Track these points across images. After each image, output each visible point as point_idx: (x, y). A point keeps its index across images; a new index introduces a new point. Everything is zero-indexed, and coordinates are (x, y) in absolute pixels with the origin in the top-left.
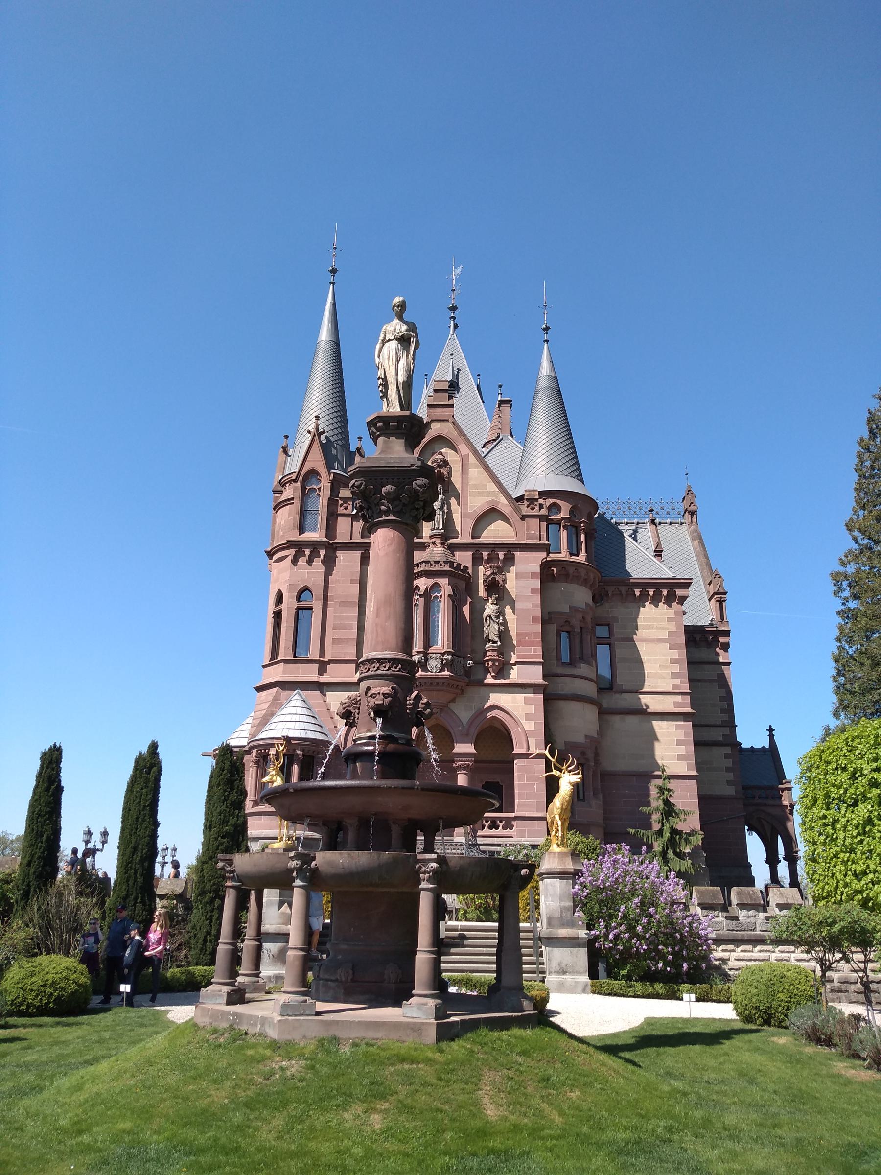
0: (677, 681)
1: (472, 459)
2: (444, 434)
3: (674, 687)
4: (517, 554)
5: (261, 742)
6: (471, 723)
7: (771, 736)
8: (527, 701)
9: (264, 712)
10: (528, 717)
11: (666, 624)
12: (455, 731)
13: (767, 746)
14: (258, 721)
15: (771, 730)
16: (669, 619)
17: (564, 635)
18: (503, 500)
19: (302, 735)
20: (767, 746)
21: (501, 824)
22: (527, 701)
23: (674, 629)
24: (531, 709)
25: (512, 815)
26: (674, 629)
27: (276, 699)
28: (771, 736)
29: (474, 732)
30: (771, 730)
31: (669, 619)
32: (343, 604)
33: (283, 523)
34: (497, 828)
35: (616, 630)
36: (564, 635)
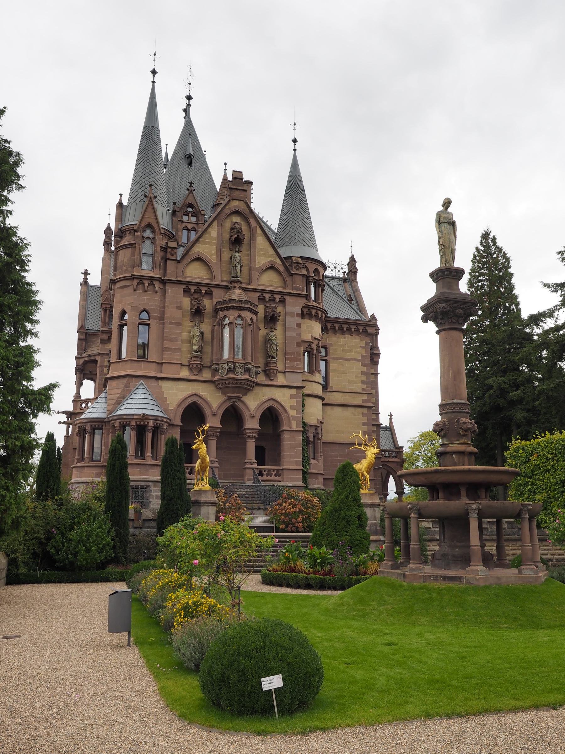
0: (365, 386)
1: (259, 231)
2: (240, 210)
3: (363, 390)
4: (288, 298)
5: (124, 417)
6: (258, 409)
7: (391, 419)
8: (292, 396)
9: (118, 396)
10: (292, 407)
11: (360, 350)
12: (246, 414)
13: (388, 425)
14: (114, 402)
15: (391, 415)
16: (362, 347)
17: (306, 354)
18: (278, 261)
19: (141, 412)
20: (388, 425)
21: (274, 473)
22: (292, 396)
23: (364, 353)
24: (294, 402)
25: (281, 468)
26: (364, 353)
27: (126, 387)
28: (391, 419)
29: (258, 415)
30: (391, 415)
31: (362, 347)
32: (171, 323)
33: (125, 260)
34: (271, 475)
35: (331, 351)
36: (306, 354)
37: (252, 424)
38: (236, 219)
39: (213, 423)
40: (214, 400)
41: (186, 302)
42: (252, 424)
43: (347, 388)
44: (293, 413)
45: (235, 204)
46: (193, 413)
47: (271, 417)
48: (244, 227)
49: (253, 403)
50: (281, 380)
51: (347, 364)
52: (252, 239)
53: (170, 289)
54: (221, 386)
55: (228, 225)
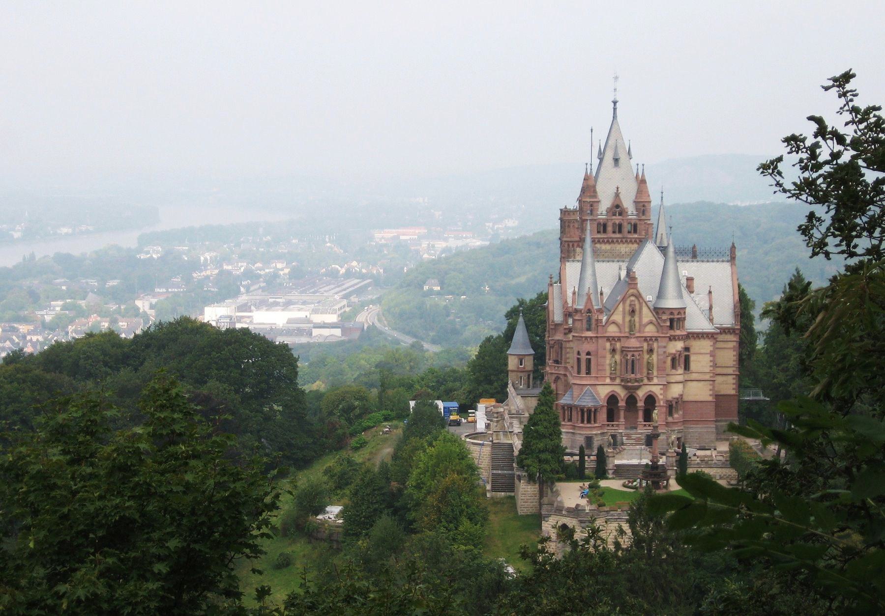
1: (644, 304)
37: (641, 404)
38: (632, 298)
39: (622, 404)
40: (622, 393)
41: (608, 345)
42: (641, 404)
43: (701, 370)
44: (661, 397)
45: (631, 291)
46: (612, 399)
47: (651, 400)
48: (637, 302)
49: (641, 394)
50: (655, 381)
51: (701, 356)
52: (641, 309)
53: (600, 341)
54: (626, 388)
55: (628, 302)
